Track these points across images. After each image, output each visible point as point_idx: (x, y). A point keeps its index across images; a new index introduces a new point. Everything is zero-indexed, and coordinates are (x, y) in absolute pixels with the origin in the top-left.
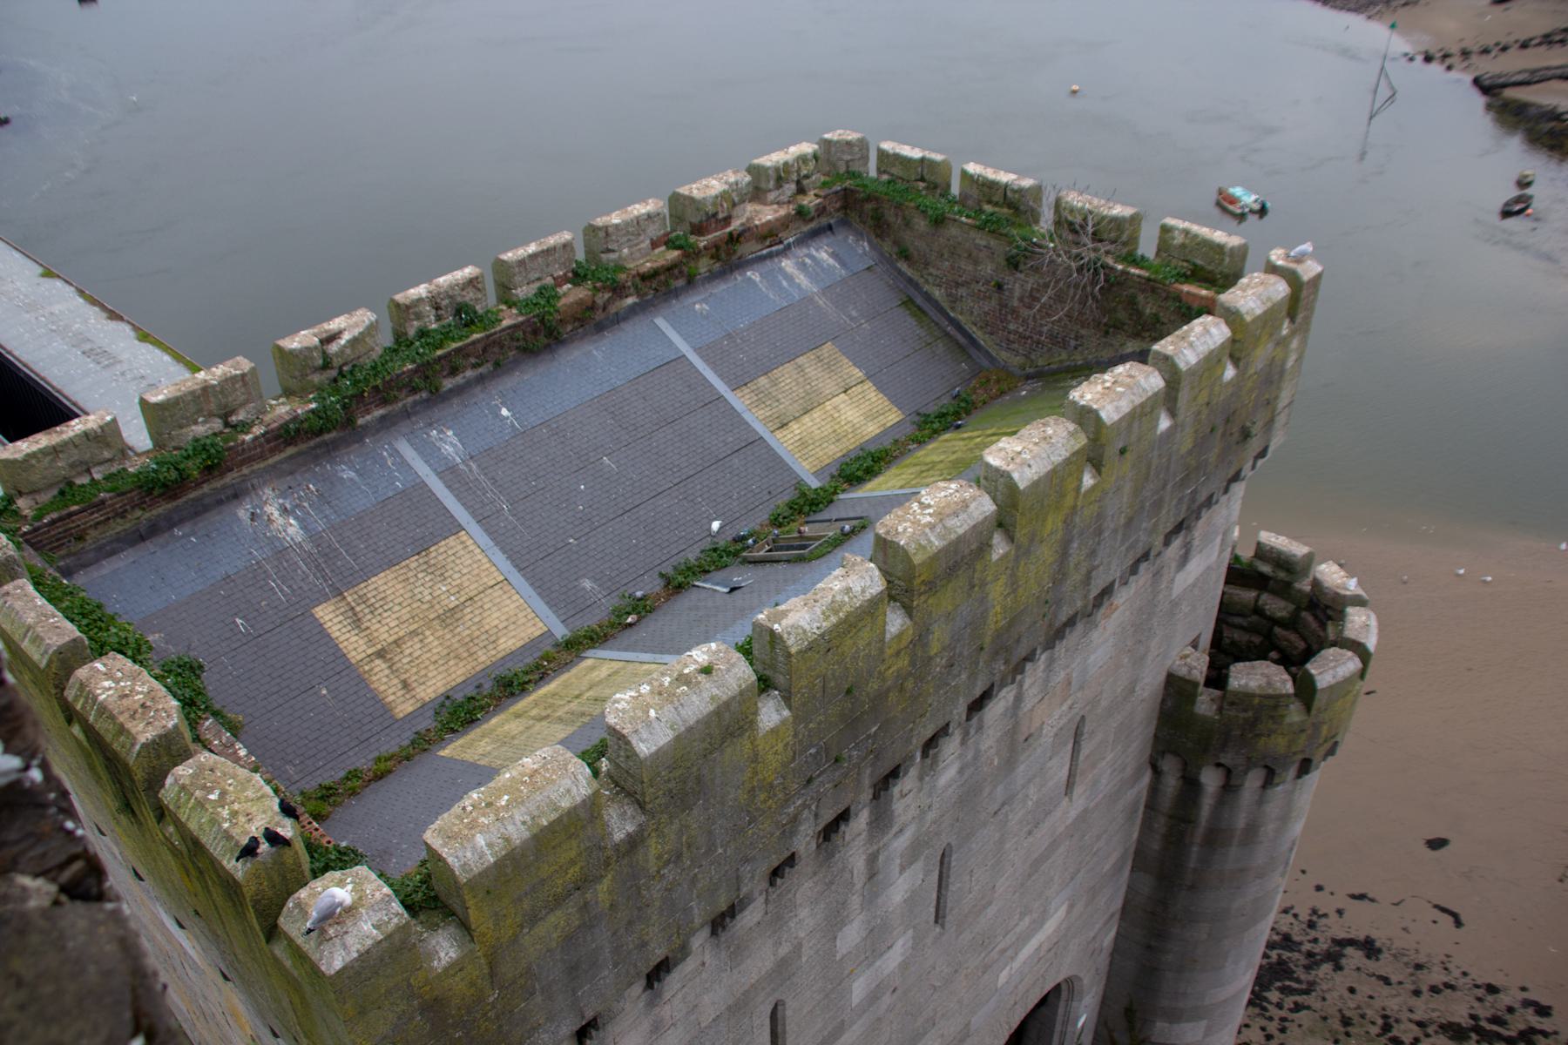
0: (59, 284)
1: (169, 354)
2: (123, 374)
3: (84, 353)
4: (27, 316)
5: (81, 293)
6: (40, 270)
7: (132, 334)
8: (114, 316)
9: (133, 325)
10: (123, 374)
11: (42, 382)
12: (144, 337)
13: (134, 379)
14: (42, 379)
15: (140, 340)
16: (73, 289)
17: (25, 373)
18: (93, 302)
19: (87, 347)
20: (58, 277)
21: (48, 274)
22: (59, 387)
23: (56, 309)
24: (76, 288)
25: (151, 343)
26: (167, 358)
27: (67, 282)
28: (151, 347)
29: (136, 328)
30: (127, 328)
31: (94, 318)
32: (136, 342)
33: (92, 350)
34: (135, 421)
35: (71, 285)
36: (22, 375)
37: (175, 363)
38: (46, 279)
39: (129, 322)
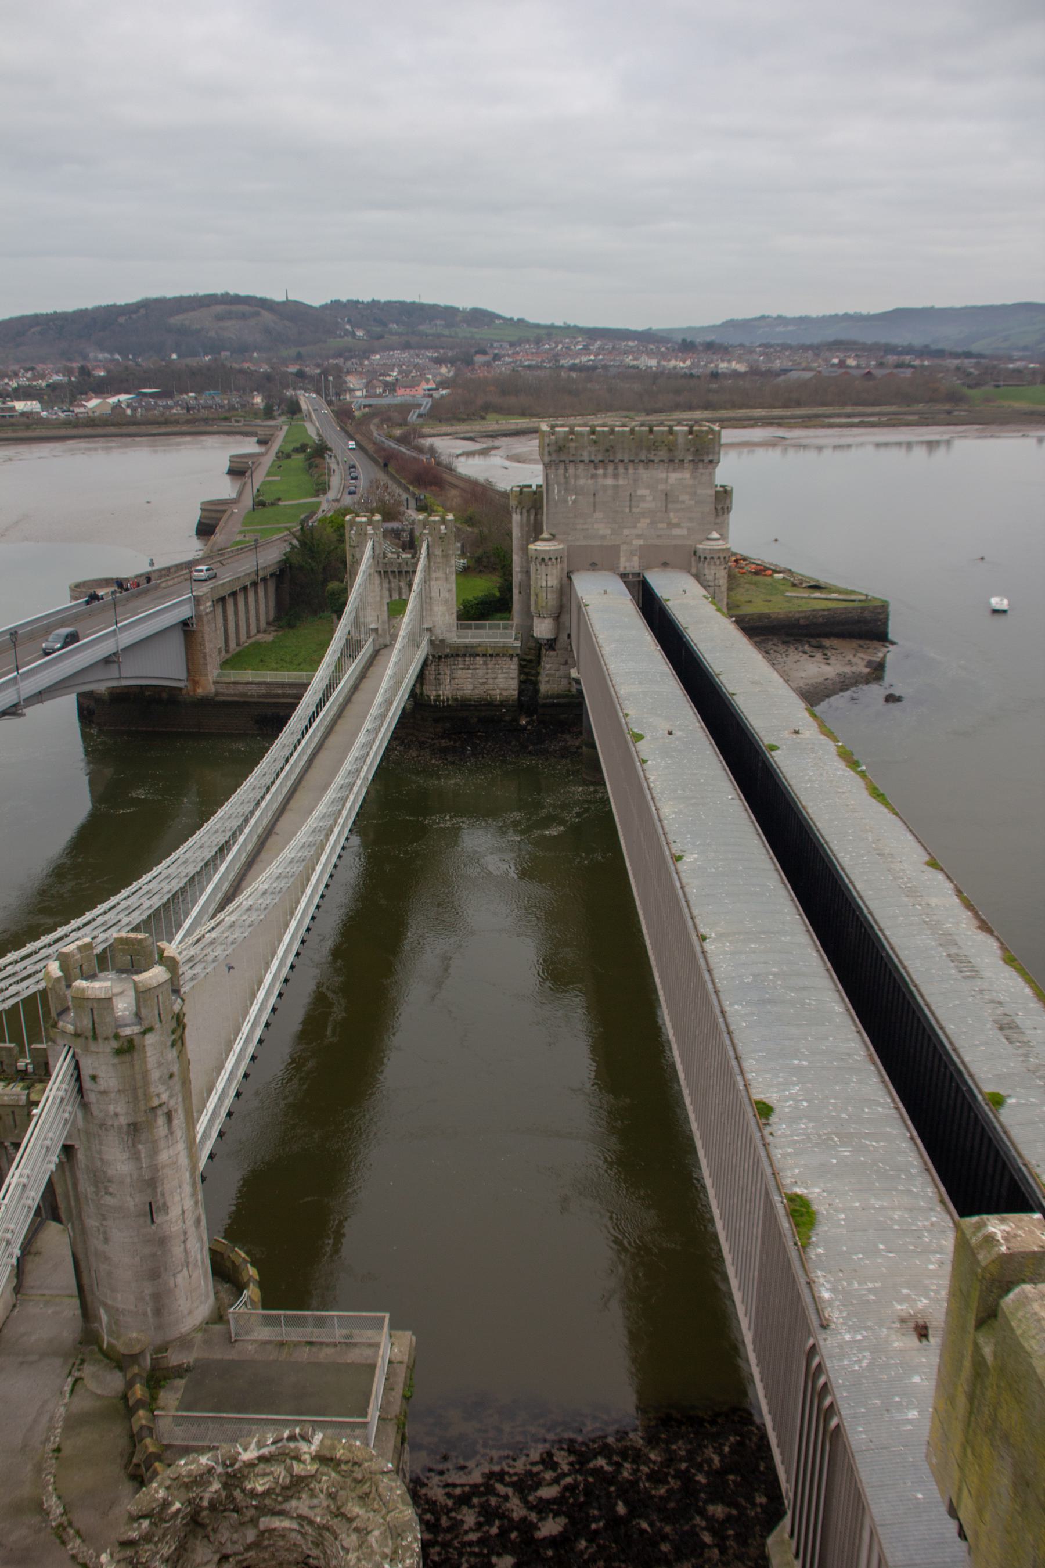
0: (941, 876)
1: (1031, 987)
2: (981, 991)
3: (949, 955)
4: (906, 899)
5: (959, 892)
6: (927, 858)
7: (999, 952)
8: (985, 927)
9: (1002, 943)
10: (981, 991)
11: (903, 971)
12: (1010, 960)
13: (992, 1001)
14: (904, 968)
15: (1006, 963)
16: (951, 886)
17: (888, 954)
18: (969, 906)
19: (954, 950)
20: (942, 870)
21: (933, 864)
22: (917, 982)
23: (934, 901)
24: (956, 887)
25: (1016, 969)
26: (1028, 991)
27: (948, 877)
28: (1015, 973)
29: (1003, 948)
30: (995, 945)
31: (963, 924)
32: (1001, 962)
33: (957, 955)
34: (983, 1048)
35: (952, 882)
36: (884, 955)
37: (1035, 999)
38: (930, 869)
39: (998, 939)
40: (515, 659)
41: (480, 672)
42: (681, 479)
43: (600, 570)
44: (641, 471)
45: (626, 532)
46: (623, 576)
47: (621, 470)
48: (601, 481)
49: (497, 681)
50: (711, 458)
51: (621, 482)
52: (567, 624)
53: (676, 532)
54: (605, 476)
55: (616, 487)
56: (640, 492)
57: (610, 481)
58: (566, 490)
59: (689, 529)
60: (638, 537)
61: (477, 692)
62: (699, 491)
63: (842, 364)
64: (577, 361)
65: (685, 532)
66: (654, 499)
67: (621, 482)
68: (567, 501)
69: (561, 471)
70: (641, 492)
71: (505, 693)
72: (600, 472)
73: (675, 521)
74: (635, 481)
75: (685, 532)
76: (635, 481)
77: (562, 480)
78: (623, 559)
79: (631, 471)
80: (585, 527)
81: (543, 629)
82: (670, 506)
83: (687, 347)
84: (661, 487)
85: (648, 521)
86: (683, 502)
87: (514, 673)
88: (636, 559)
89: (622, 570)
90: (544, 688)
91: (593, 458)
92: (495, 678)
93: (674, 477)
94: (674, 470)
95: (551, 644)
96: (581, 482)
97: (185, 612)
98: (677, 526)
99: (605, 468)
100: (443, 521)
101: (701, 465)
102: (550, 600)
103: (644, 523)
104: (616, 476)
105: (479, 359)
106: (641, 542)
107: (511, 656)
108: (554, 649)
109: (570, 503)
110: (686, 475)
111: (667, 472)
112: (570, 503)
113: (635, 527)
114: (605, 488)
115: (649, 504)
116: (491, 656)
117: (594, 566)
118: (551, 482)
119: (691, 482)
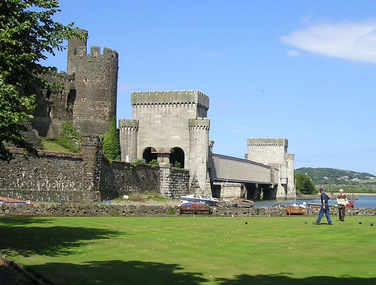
40: (240, 187)
41: (232, 190)
45: (265, 160)
48: (260, 149)
49: (236, 192)
50: (283, 144)
51: (264, 149)
53: (276, 160)
54: (260, 148)
55: (263, 150)
56: (268, 152)
57: (261, 149)
58: (252, 151)
59: (279, 160)
60: (268, 161)
61: (231, 195)
62: (280, 152)
65: (278, 160)
66: (271, 153)
68: (252, 153)
71: (238, 195)
73: (276, 158)
74: (267, 149)
75: (278, 160)
76: (267, 149)
77: (251, 149)
80: (256, 159)
84: (272, 150)
85: (270, 158)
86: (277, 154)
91: (258, 144)
92: (235, 192)
96: (255, 149)
98: (276, 159)
103: (269, 158)
104: (263, 148)
106: (268, 163)
109: (253, 154)
112: (253, 154)
113: (266, 159)
114: (260, 150)
115: (270, 154)
118: (249, 149)
119: (279, 149)
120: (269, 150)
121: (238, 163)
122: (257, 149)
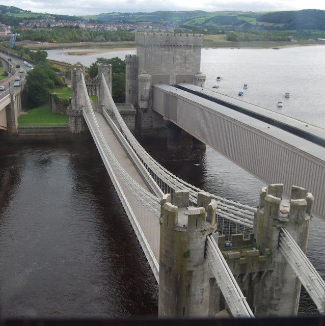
40: (134, 116)
42: (190, 52)
43: (163, 84)
44: (177, 49)
45: (172, 70)
46: (172, 86)
47: (171, 49)
51: (170, 53)
52: (151, 103)
53: (188, 71)
54: (165, 50)
55: (169, 55)
57: (167, 53)
60: (175, 72)
63: (148, 27)
64: (57, 25)
66: (181, 59)
67: (170, 53)
69: (150, 49)
70: (177, 56)
72: (163, 49)
73: (188, 67)
74: (175, 52)
75: (191, 71)
76: (175, 52)
78: (171, 80)
79: (174, 49)
81: (143, 105)
82: (186, 61)
83: (92, 21)
84: (183, 55)
87: (134, 121)
88: (175, 80)
89: (171, 84)
90: (143, 126)
93: (188, 51)
94: (188, 49)
95: (145, 111)
97: (8, 101)
98: (188, 68)
99: (165, 48)
100: (109, 67)
101: (196, 47)
102: (146, 95)
103: (178, 67)
104: (169, 51)
105: (20, 24)
107: (133, 115)
108: (147, 112)
110: (192, 51)
111: (186, 49)
115: (180, 61)
116: (126, 115)
117: (161, 83)
120: (179, 55)
121: (310, 130)
122: (160, 52)
